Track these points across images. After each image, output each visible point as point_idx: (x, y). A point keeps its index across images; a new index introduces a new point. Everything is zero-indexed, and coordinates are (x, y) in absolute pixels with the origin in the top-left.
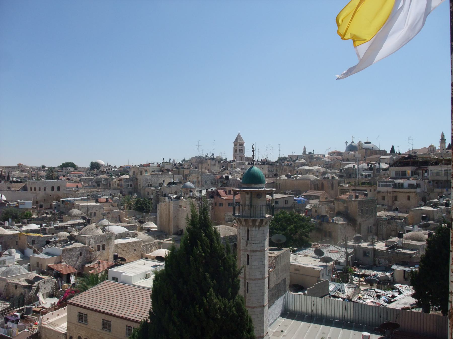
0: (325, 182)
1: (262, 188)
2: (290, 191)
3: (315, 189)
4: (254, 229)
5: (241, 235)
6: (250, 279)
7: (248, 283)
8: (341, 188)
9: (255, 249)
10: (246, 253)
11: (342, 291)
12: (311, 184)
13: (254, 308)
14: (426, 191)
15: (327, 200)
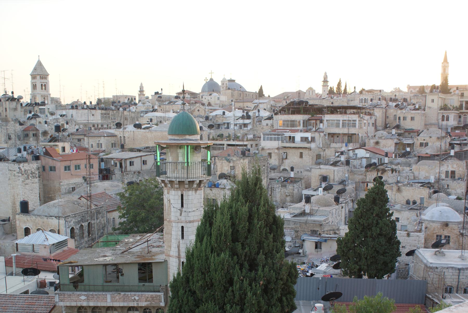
4: (190, 192)
5: (172, 201)
9: (192, 219)
14: (321, 146)
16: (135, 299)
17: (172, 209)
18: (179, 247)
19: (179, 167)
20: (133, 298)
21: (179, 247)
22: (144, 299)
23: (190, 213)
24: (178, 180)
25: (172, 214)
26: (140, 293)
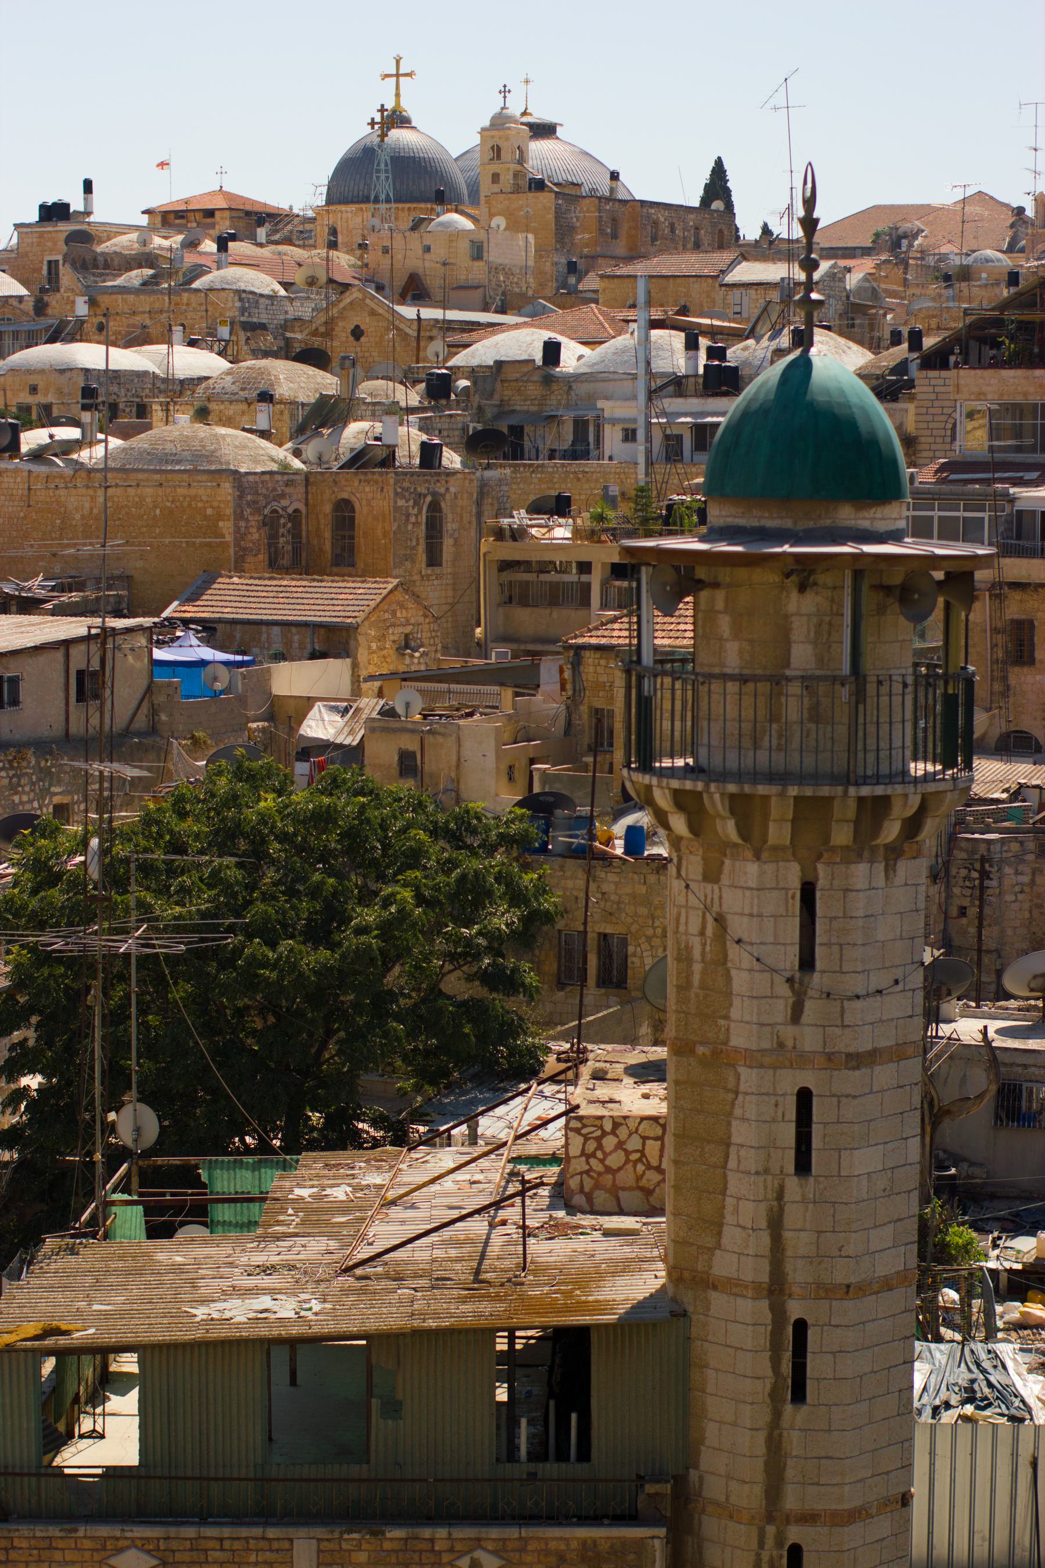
0: (373, 500)
1: (895, 537)
2: (36, 586)
3: (275, 565)
5: (738, 926)
6: (825, 1291)
7: (801, 1327)
8: (509, 551)
9: (864, 1045)
10: (790, 1082)
11: (1002, 1398)
12: (239, 516)
13: (854, 1516)
15: (416, 662)
17: (740, 981)
18: (776, 1224)
19: (794, 705)
21: (776, 1224)
23: (858, 1004)
24: (793, 791)
25: (735, 1013)
26: (512, 1532)
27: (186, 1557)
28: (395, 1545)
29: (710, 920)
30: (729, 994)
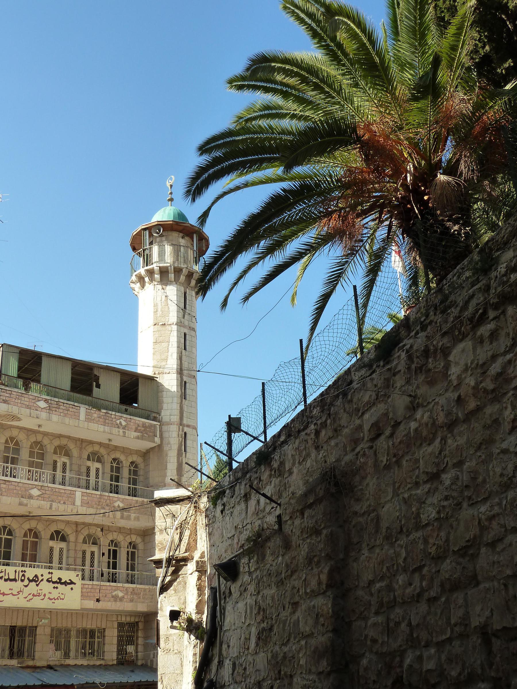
16: (120, 422)
20: (118, 422)
22: (134, 427)
25: (170, 315)
27: (55, 406)
28: (104, 414)
29: (164, 297)
30: (169, 312)
